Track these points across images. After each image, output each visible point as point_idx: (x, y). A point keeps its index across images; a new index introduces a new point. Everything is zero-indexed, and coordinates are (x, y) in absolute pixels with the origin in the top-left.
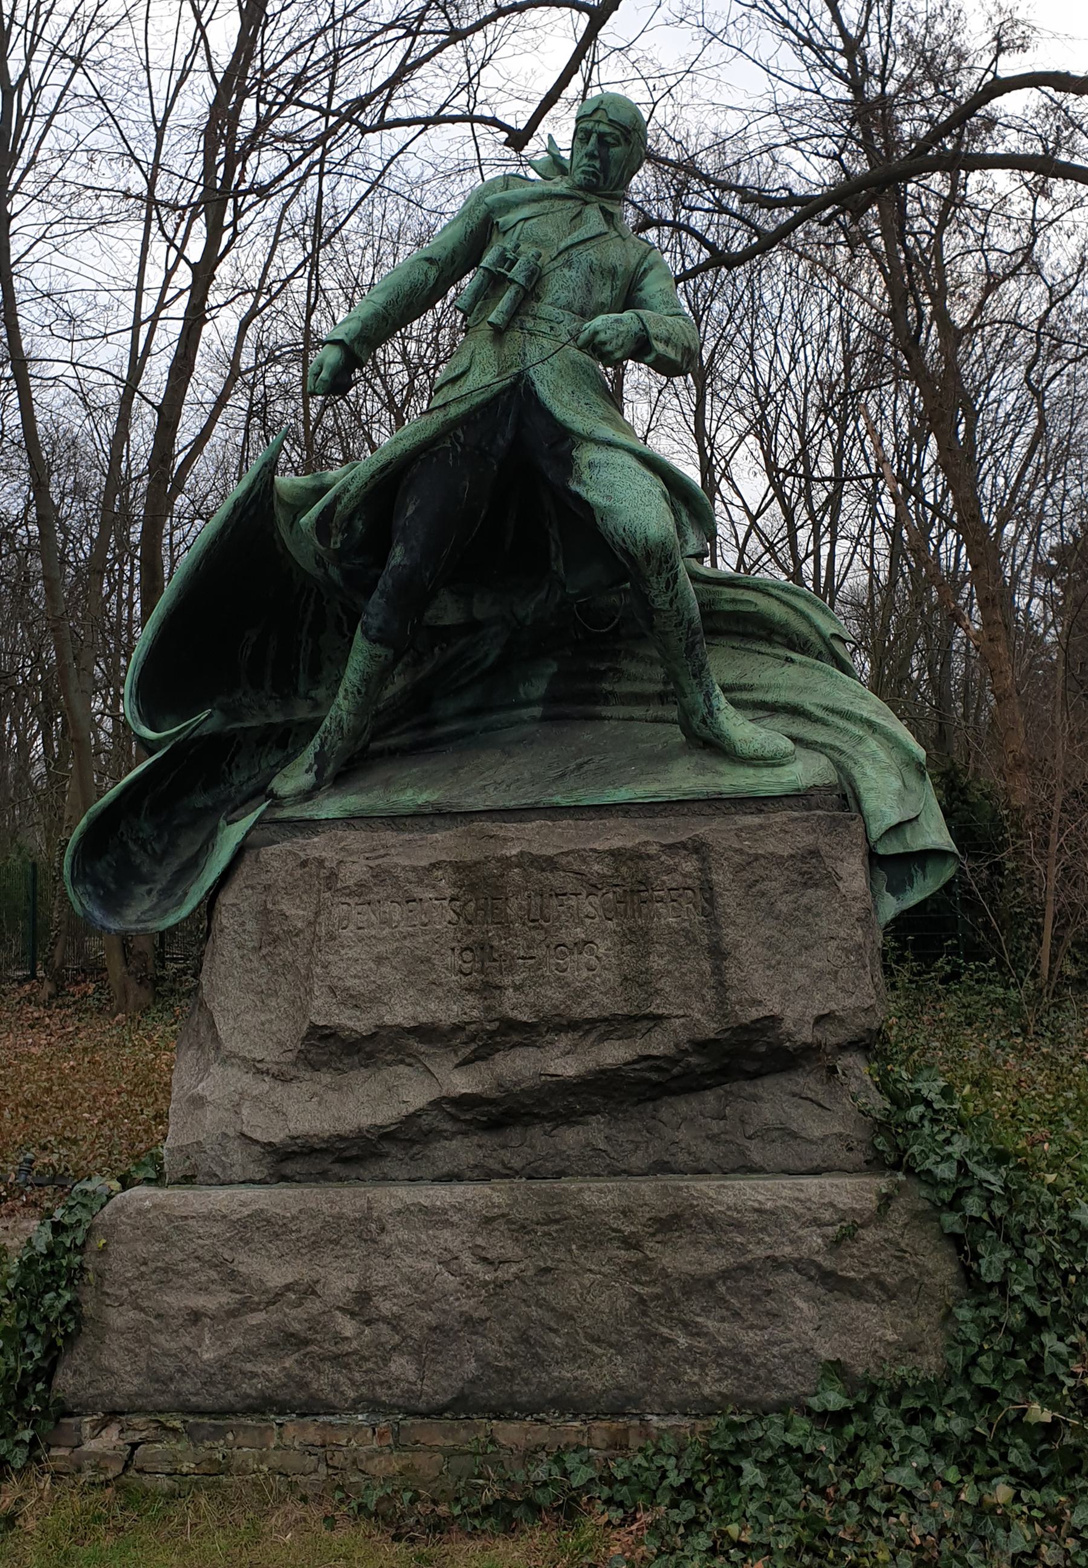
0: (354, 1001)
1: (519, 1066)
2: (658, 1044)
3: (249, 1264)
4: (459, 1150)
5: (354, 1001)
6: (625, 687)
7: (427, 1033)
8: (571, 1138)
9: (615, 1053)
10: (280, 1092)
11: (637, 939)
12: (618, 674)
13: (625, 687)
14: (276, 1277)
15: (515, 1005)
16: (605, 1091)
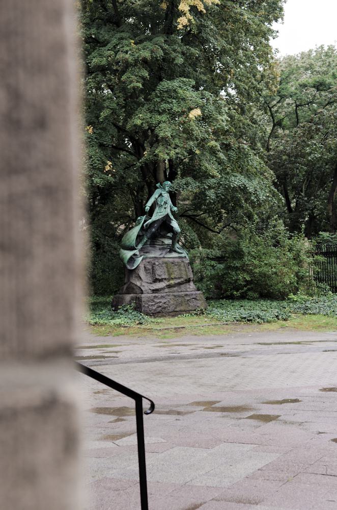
0: (160, 276)
1: (172, 282)
2: (182, 280)
3: (155, 300)
4: (167, 290)
5: (160, 276)
6: (157, 243)
7: (165, 279)
8: (175, 289)
9: (179, 281)
10: (151, 285)
11: (180, 270)
12: (157, 242)
13: (157, 243)
14: (158, 301)
15: (173, 276)
16: (179, 284)
